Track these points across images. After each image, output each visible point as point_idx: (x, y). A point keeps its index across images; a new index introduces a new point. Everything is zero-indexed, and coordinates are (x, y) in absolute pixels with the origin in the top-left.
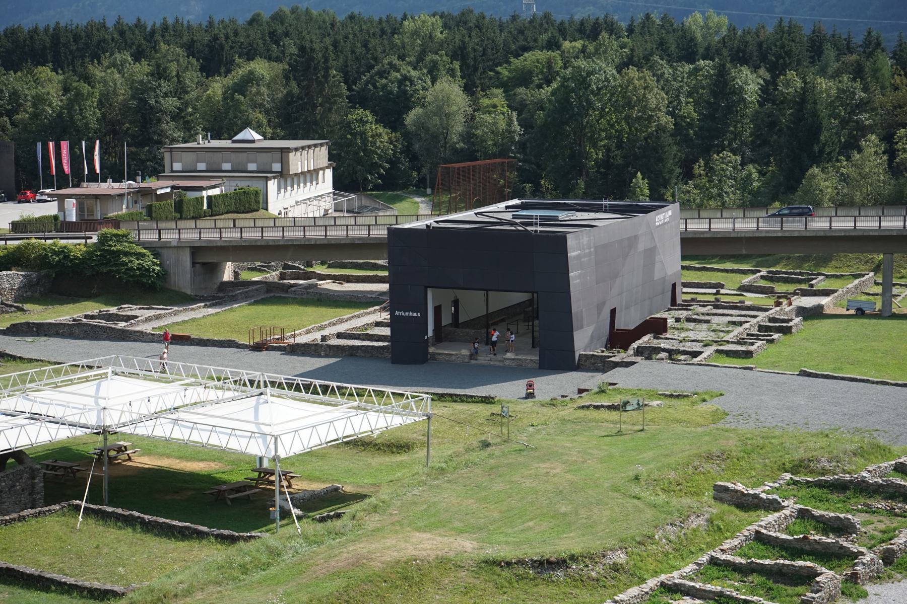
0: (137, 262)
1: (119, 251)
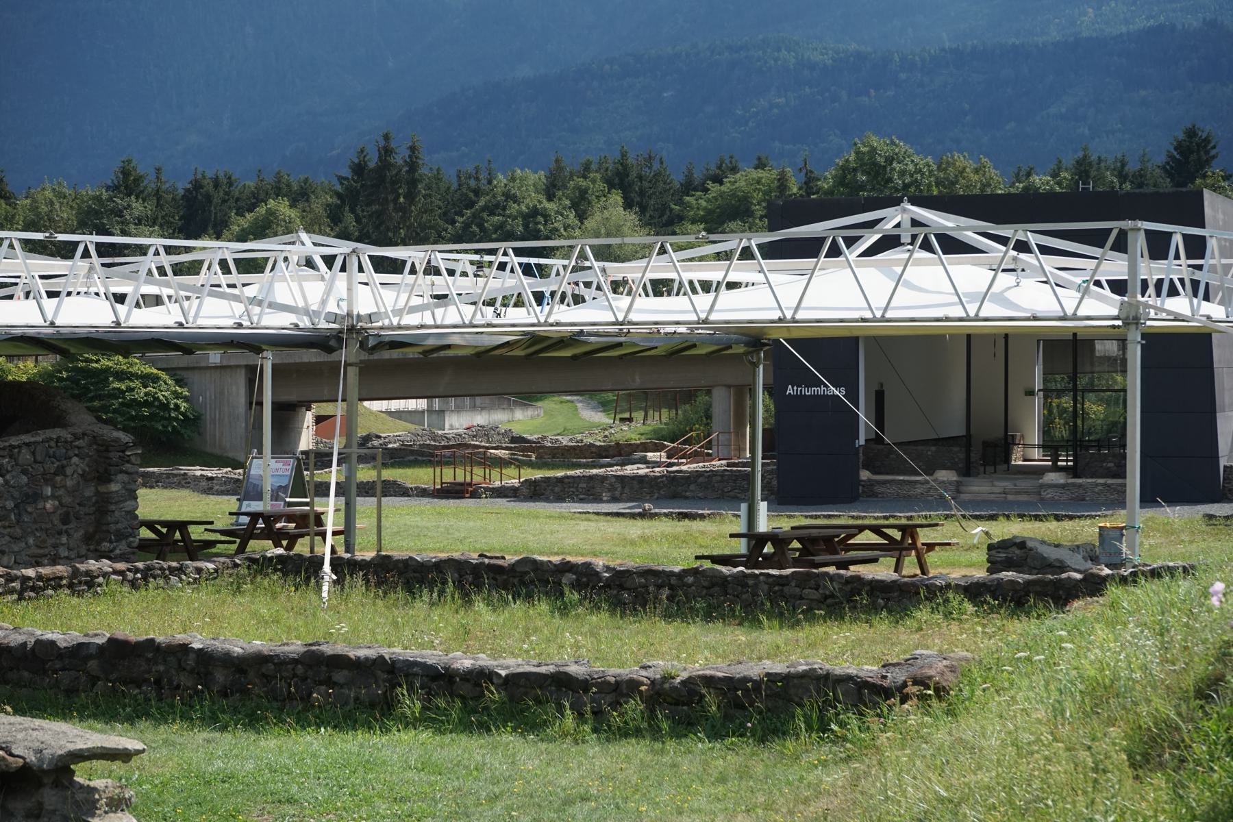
0: (144, 390)
1: (107, 370)
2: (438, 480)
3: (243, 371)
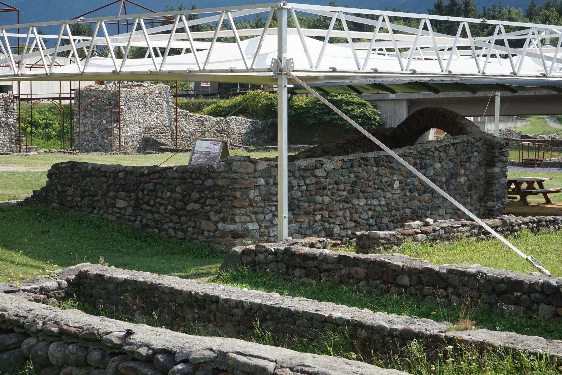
0: (359, 110)
2: (521, 158)
3: (406, 102)
